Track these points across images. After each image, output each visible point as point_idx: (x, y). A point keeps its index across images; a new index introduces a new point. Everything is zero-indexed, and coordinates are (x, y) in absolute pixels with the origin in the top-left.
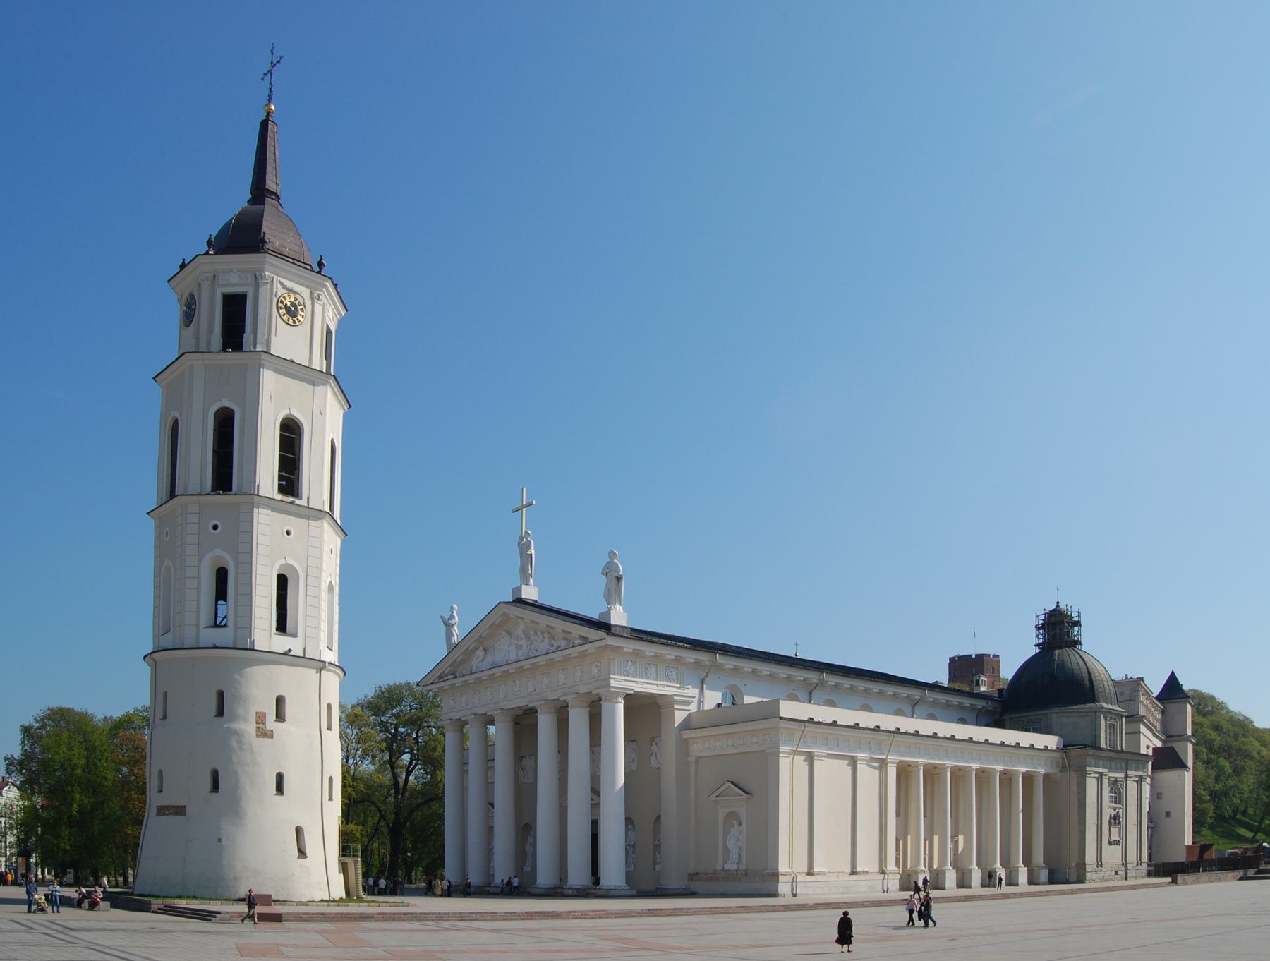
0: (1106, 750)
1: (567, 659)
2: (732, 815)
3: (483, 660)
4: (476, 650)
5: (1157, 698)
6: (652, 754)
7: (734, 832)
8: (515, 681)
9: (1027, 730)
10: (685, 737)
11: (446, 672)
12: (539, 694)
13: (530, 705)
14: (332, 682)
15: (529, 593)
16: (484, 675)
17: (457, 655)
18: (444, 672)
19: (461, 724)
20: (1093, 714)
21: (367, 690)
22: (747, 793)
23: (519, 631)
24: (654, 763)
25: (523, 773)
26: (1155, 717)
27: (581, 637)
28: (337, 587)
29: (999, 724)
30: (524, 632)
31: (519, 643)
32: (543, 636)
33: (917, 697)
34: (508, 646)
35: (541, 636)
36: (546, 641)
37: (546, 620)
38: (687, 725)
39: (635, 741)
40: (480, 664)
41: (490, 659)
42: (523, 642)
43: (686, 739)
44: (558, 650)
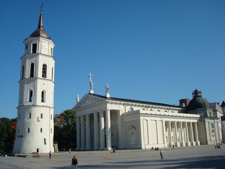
0: (209, 117)
1: (99, 104)
2: (132, 133)
7: (133, 136)
9: (192, 114)
14: (52, 111)
15: (92, 92)
16: (84, 108)
19: (80, 117)
21: (61, 111)
24: (117, 123)
37: (95, 97)
38: (123, 115)
41: (85, 105)
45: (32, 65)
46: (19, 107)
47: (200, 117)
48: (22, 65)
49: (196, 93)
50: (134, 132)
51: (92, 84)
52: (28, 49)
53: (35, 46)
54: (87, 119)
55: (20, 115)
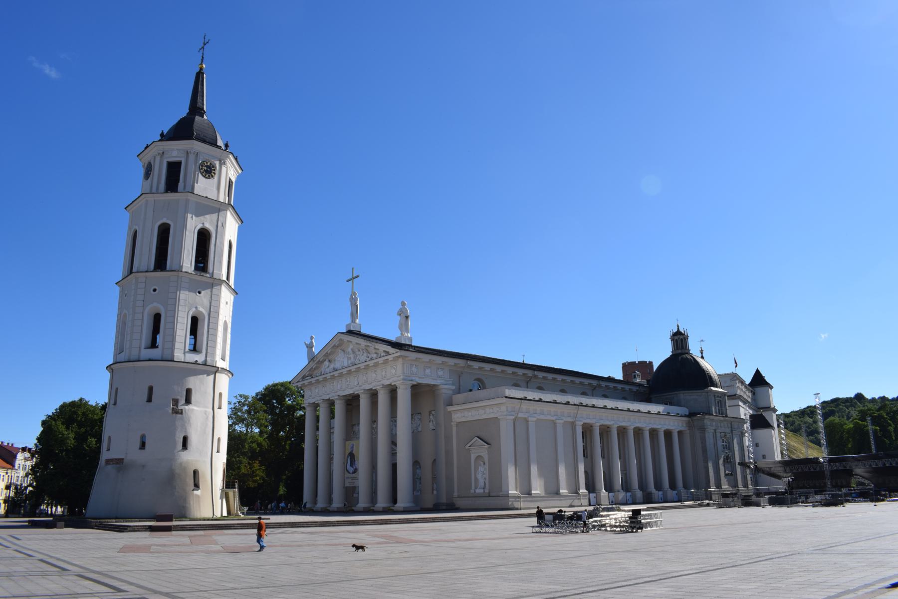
1: (376, 365)
2: (479, 458)
5: (749, 385)
6: (430, 421)
7: (481, 469)
8: (347, 379)
10: (449, 410)
11: (306, 375)
12: (361, 386)
13: (356, 393)
17: (313, 365)
18: (305, 375)
19: (316, 406)
20: (706, 394)
21: (254, 388)
22: (488, 444)
23: (349, 350)
26: (749, 397)
27: (385, 351)
28: (230, 324)
29: (648, 400)
31: (349, 356)
33: (594, 384)
34: (343, 358)
36: (365, 354)
39: (420, 413)
41: (332, 366)
42: (352, 356)
43: (450, 412)
44: (371, 359)
45: (164, 232)
46: (112, 366)
47: (687, 414)
48: (130, 228)
49: (679, 339)
50: (485, 456)
51: (358, 304)
52: (152, 178)
53: (174, 169)
54: (339, 409)
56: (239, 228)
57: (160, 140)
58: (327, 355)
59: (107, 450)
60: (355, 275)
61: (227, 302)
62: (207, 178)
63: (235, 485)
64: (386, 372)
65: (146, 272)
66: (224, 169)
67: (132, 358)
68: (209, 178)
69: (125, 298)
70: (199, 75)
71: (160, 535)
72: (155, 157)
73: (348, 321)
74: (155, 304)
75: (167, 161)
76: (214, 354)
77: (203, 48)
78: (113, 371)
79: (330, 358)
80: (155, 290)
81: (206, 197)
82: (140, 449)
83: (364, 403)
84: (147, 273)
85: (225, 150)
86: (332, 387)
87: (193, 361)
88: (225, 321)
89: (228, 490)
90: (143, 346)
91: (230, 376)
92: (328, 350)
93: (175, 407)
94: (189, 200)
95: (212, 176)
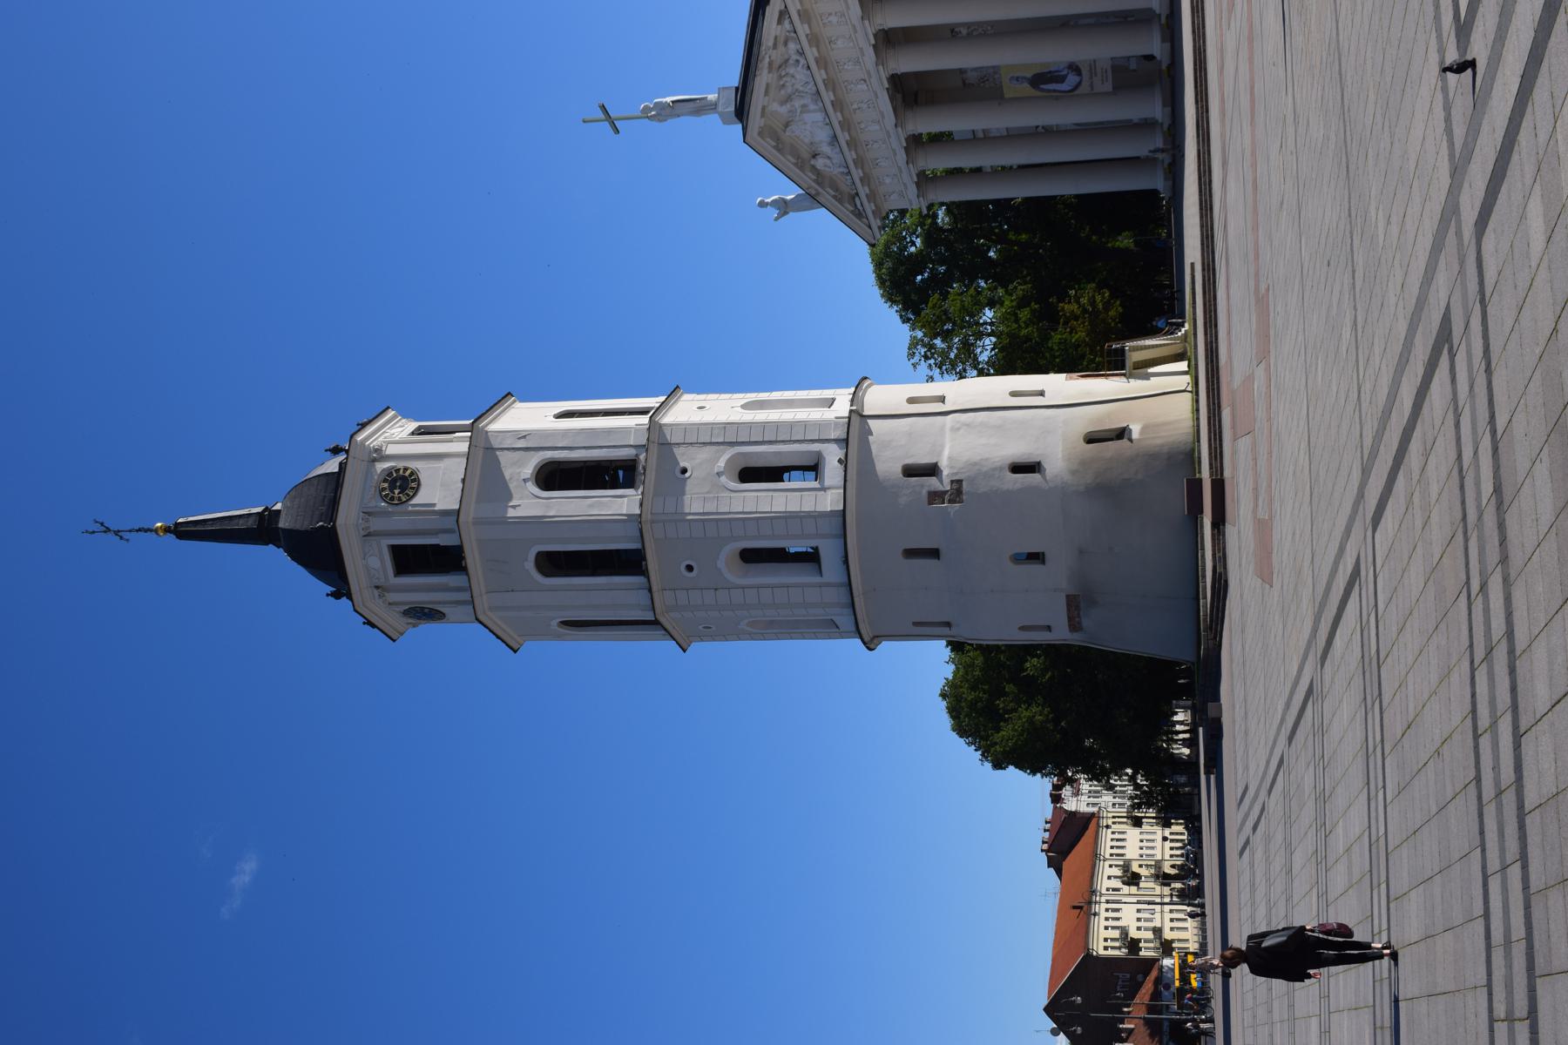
1: (814, 40)
3: (829, 158)
4: (816, 169)
8: (855, 110)
11: (852, 209)
12: (869, 73)
13: (887, 86)
17: (826, 195)
18: (852, 212)
23: (783, 110)
25: (987, 80)
27: (780, 22)
28: (749, 395)
30: (783, 103)
31: (799, 111)
32: (784, 76)
35: (784, 79)
36: (791, 70)
40: (834, 161)
41: (826, 149)
42: (797, 103)
44: (801, 53)
45: (556, 563)
46: (866, 639)
48: (559, 637)
51: (669, 99)
52: (440, 603)
53: (410, 559)
54: (927, 122)
55: (916, 624)
56: (522, 400)
57: (350, 597)
58: (801, 165)
59: (1050, 631)
60: (602, 116)
61: (700, 408)
62: (419, 485)
63: (1116, 349)
64: (830, 14)
65: (650, 590)
66: (391, 450)
67: (845, 599)
68: (417, 481)
69: (714, 629)
70: (184, 532)
71: (1233, 501)
72: (390, 604)
73: (713, 119)
74: (721, 564)
75: (395, 576)
76: (821, 425)
77: (117, 533)
78: (877, 637)
79: (805, 155)
80: (690, 568)
81: (463, 481)
82: (1043, 562)
83: (910, 62)
84: (654, 588)
85: (347, 452)
86: (876, 146)
87: (840, 469)
88: (744, 407)
89: (1129, 364)
90: (817, 579)
91: (866, 383)
92: (788, 161)
93: (947, 497)
94: (473, 518)
95: (412, 474)
